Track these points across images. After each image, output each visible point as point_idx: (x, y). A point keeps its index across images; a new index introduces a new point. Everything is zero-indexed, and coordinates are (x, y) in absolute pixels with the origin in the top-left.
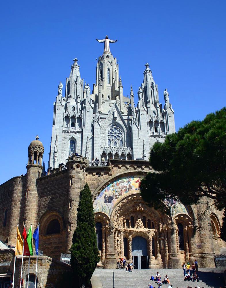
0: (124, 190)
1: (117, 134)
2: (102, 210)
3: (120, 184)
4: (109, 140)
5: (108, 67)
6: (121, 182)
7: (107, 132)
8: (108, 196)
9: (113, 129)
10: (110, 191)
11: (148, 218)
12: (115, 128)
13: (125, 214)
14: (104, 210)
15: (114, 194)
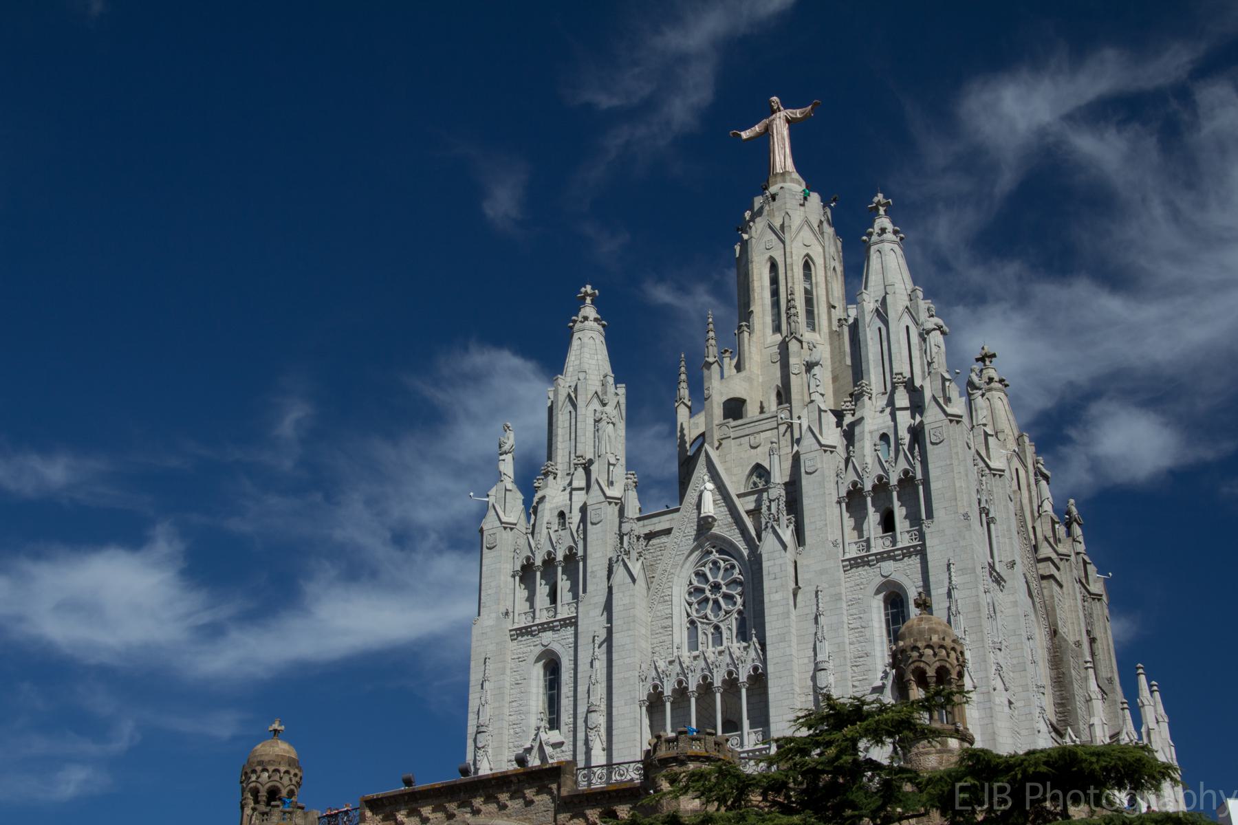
1: (724, 589)
4: (692, 622)
7: (679, 592)
9: (707, 570)
12: (715, 563)
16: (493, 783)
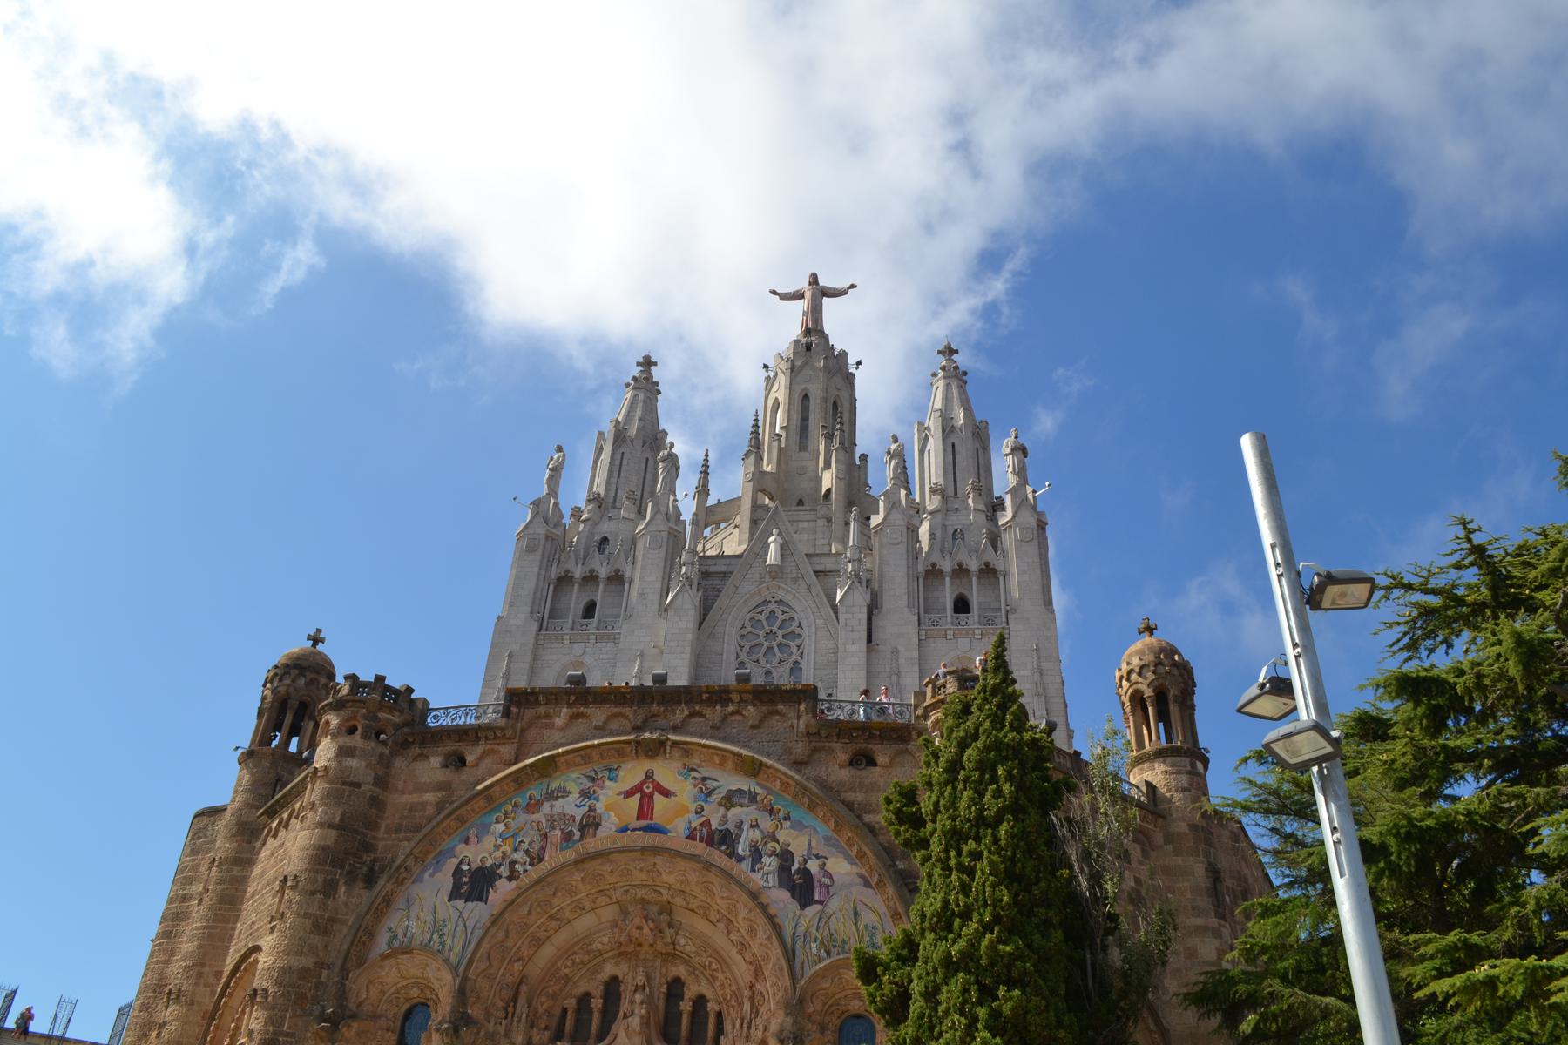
0: (557, 832)
2: (427, 937)
3: (546, 806)
5: (802, 387)
6: (552, 796)
8: (474, 867)
9: (763, 617)
10: (489, 842)
11: (691, 991)
12: (772, 612)
13: (569, 963)
14: (441, 936)
15: (504, 855)
16: (704, 697)
